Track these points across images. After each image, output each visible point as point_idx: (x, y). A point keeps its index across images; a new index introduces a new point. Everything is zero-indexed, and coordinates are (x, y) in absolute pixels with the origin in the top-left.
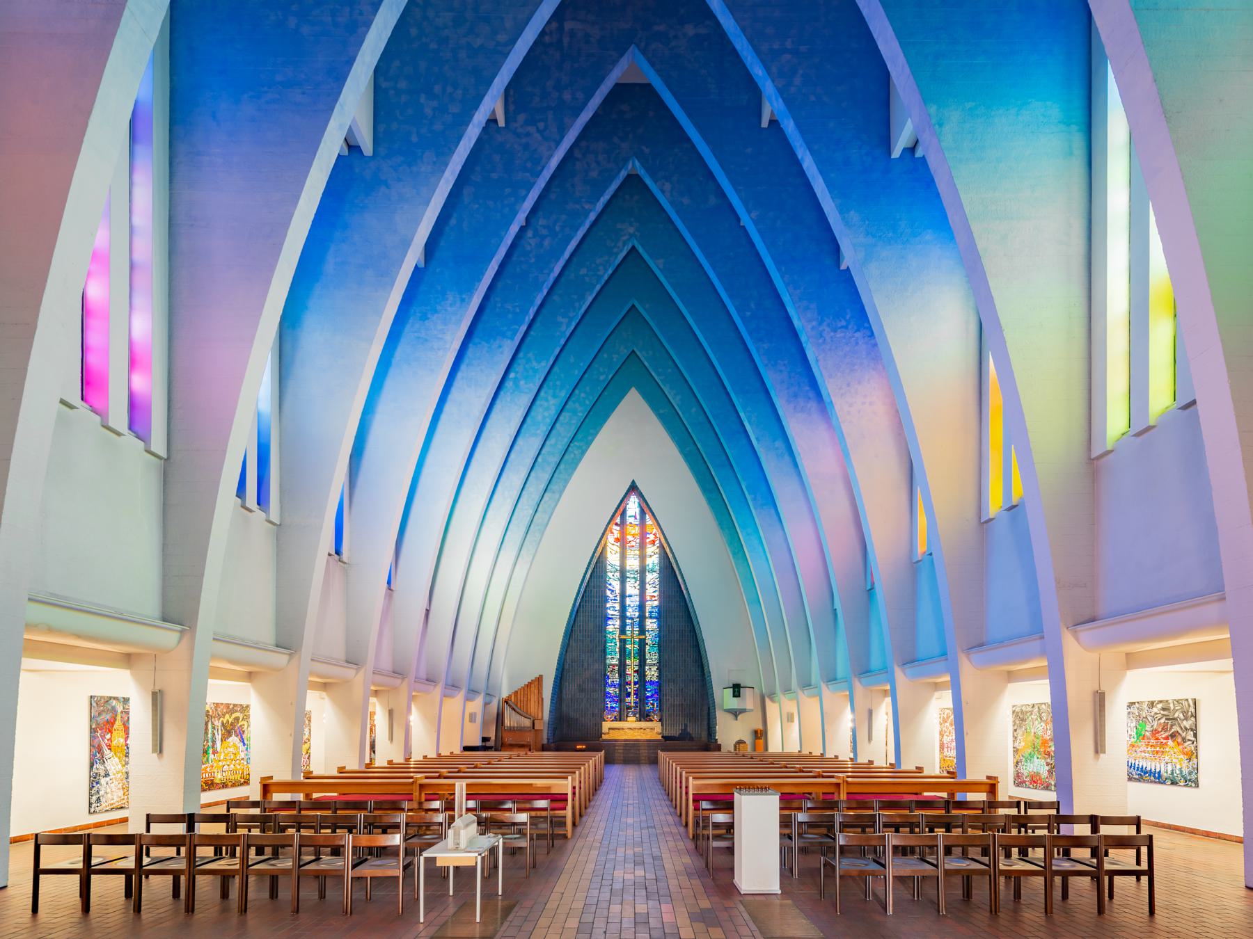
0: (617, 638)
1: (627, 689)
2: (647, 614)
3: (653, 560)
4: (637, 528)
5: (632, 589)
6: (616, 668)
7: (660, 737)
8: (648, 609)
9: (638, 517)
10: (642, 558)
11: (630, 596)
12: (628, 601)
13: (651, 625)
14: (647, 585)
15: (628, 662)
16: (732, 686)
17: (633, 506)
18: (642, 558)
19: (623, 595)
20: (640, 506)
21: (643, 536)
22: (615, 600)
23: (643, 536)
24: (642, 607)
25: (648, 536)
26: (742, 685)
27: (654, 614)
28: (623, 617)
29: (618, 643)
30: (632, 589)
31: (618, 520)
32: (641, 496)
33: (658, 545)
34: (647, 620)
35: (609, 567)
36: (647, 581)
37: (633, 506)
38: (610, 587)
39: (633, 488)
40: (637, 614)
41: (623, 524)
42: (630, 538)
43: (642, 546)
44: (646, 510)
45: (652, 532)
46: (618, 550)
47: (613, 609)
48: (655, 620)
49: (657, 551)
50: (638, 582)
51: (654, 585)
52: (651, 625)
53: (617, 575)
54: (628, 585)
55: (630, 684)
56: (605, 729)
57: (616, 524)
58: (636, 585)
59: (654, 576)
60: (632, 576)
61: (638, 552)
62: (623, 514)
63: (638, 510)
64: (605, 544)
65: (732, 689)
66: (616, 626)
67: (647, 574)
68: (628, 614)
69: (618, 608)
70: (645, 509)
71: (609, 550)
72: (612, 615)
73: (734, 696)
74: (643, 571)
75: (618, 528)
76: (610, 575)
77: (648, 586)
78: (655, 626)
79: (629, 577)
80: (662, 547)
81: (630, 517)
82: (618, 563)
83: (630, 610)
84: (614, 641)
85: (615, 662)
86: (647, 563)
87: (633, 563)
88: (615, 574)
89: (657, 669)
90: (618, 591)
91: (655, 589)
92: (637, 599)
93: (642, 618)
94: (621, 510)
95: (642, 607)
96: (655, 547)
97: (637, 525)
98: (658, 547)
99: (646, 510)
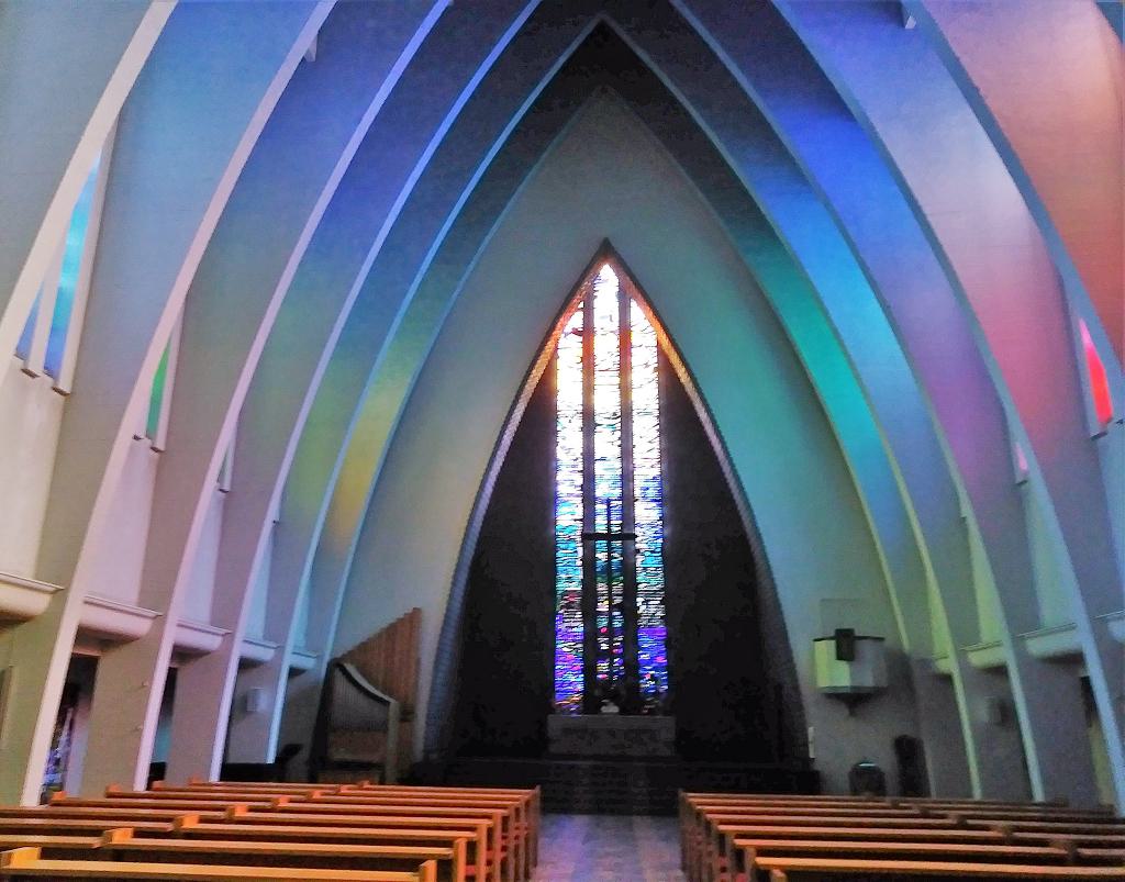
0: (579, 539)
2: (638, 493)
3: (647, 395)
5: (606, 444)
6: (577, 600)
10: (625, 390)
11: (603, 459)
12: (599, 468)
13: (647, 514)
16: (833, 634)
18: (625, 390)
19: (589, 457)
24: (626, 478)
26: (857, 633)
27: (652, 493)
28: (589, 498)
29: (580, 550)
30: (606, 444)
40: (618, 492)
43: (624, 368)
47: (567, 482)
48: (654, 504)
50: (618, 434)
52: (647, 513)
53: (578, 422)
54: (597, 437)
65: (833, 642)
68: (599, 493)
69: (579, 480)
72: (570, 495)
73: (840, 657)
74: (626, 415)
77: (636, 441)
81: (603, 317)
84: (573, 545)
85: (576, 587)
87: (606, 401)
89: (662, 602)
91: (650, 446)
92: (618, 464)
93: (628, 500)
95: (626, 478)
96: (651, 368)
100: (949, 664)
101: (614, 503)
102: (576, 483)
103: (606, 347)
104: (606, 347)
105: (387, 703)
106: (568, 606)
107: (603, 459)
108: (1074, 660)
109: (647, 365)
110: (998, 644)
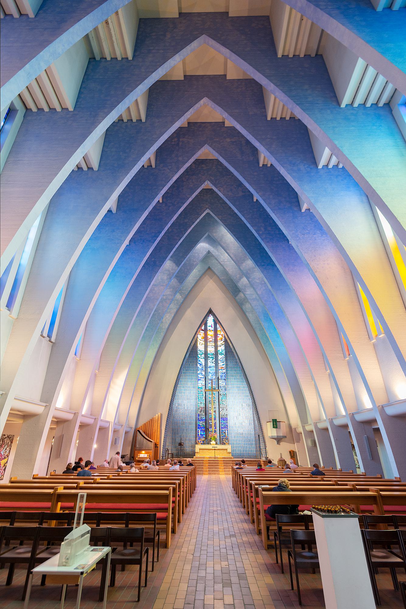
0: (203, 391)
1: (210, 423)
3: (221, 349)
4: (213, 332)
5: (211, 363)
7: (230, 456)
8: (220, 374)
9: (213, 326)
10: (216, 347)
11: (210, 367)
14: (219, 361)
15: (210, 405)
17: (210, 321)
18: (216, 347)
20: (214, 320)
21: (216, 335)
22: (202, 369)
23: (216, 335)
24: (216, 373)
25: (218, 336)
31: (203, 328)
32: (214, 315)
33: (224, 340)
34: (220, 381)
35: (199, 352)
36: (219, 359)
37: (210, 321)
38: (200, 362)
39: (210, 312)
41: (206, 330)
42: (209, 337)
43: (216, 341)
44: (217, 322)
45: (221, 333)
46: (203, 343)
49: (223, 343)
50: (214, 360)
51: (223, 361)
52: (222, 383)
55: (211, 420)
56: (197, 450)
57: (202, 330)
58: (213, 361)
59: (222, 356)
60: (211, 356)
61: (214, 344)
62: (206, 324)
63: (213, 323)
64: (197, 339)
66: (203, 384)
67: (219, 355)
69: (204, 373)
70: (216, 321)
71: (198, 343)
72: (201, 378)
75: (203, 332)
76: (199, 356)
78: (224, 383)
79: (209, 357)
80: (226, 341)
82: (203, 350)
83: (210, 375)
86: (218, 350)
88: (202, 356)
90: (204, 365)
91: (223, 364)
94: (204, 322)
96: (223, 341)
97: (213, 330)
98: (224, 341)
99: (217, 322)
100: (300, 430)
101: (213, 380)
102: (203, 374)
103: (211, 334)
104: (211, 334)
105: (152, 442)
106: (201, 411)
107: (210, 367)
108: (326, 429)
109: (222, 340)
110: (311, 424)
